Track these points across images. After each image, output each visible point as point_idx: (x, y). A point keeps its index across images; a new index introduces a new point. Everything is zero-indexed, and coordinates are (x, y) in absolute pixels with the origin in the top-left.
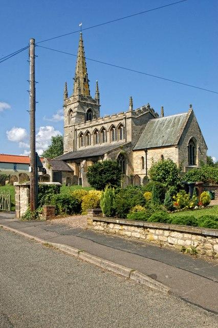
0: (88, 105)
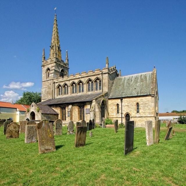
0: (62, 66)
